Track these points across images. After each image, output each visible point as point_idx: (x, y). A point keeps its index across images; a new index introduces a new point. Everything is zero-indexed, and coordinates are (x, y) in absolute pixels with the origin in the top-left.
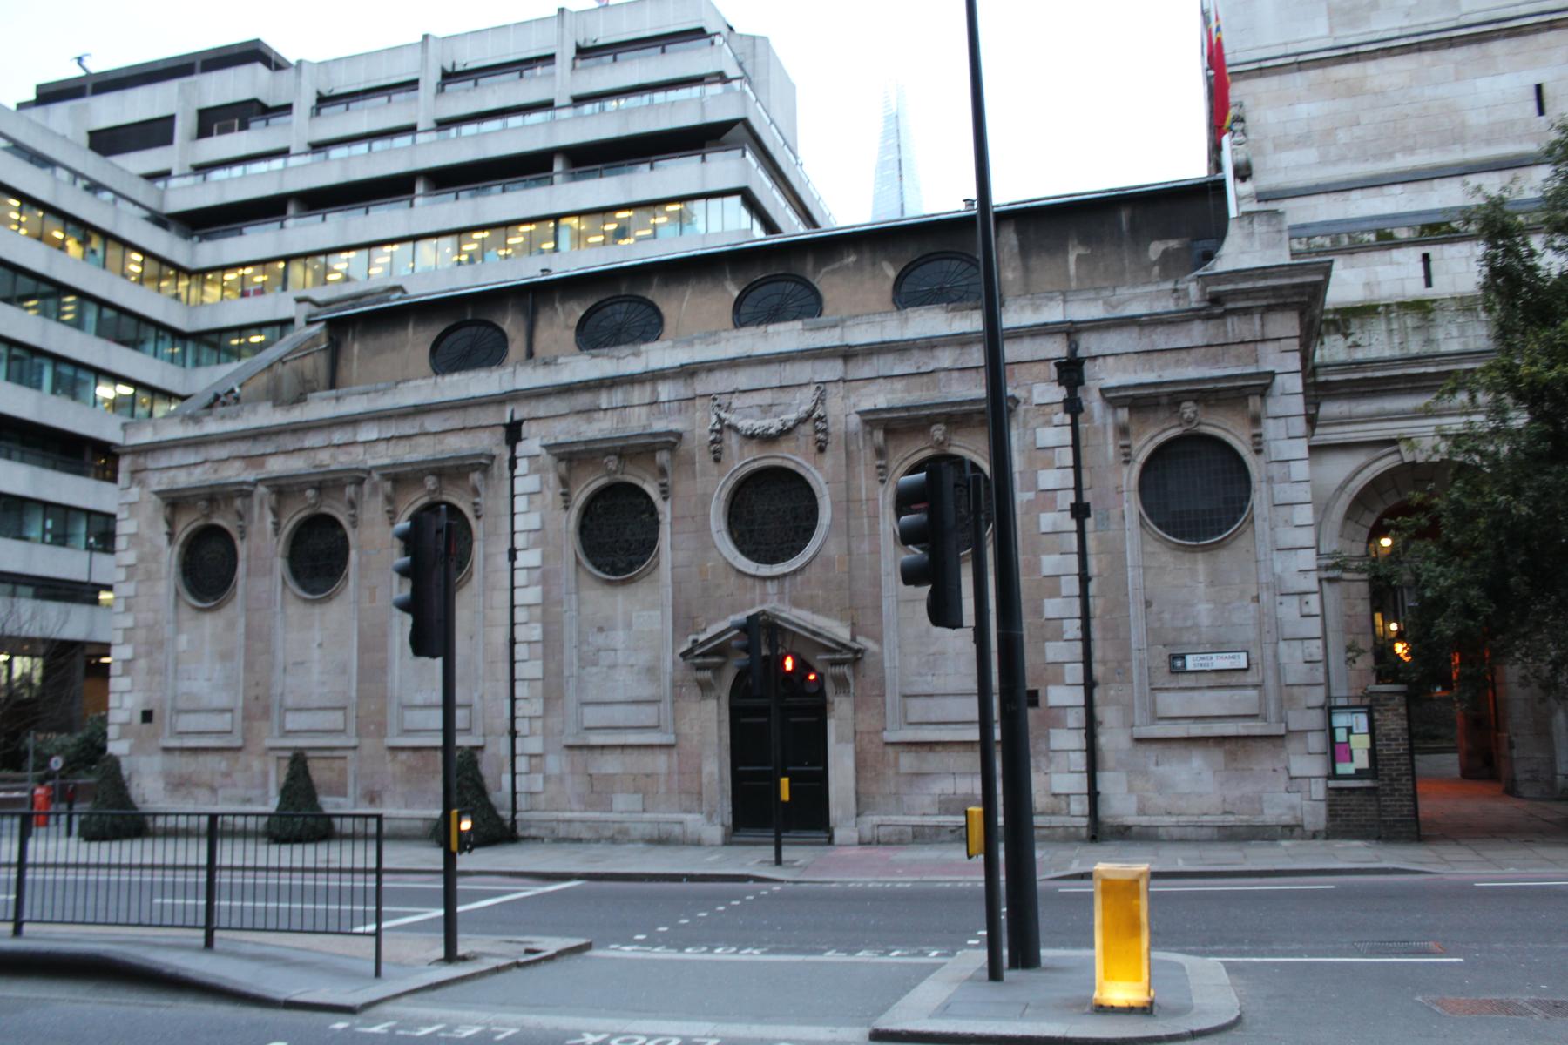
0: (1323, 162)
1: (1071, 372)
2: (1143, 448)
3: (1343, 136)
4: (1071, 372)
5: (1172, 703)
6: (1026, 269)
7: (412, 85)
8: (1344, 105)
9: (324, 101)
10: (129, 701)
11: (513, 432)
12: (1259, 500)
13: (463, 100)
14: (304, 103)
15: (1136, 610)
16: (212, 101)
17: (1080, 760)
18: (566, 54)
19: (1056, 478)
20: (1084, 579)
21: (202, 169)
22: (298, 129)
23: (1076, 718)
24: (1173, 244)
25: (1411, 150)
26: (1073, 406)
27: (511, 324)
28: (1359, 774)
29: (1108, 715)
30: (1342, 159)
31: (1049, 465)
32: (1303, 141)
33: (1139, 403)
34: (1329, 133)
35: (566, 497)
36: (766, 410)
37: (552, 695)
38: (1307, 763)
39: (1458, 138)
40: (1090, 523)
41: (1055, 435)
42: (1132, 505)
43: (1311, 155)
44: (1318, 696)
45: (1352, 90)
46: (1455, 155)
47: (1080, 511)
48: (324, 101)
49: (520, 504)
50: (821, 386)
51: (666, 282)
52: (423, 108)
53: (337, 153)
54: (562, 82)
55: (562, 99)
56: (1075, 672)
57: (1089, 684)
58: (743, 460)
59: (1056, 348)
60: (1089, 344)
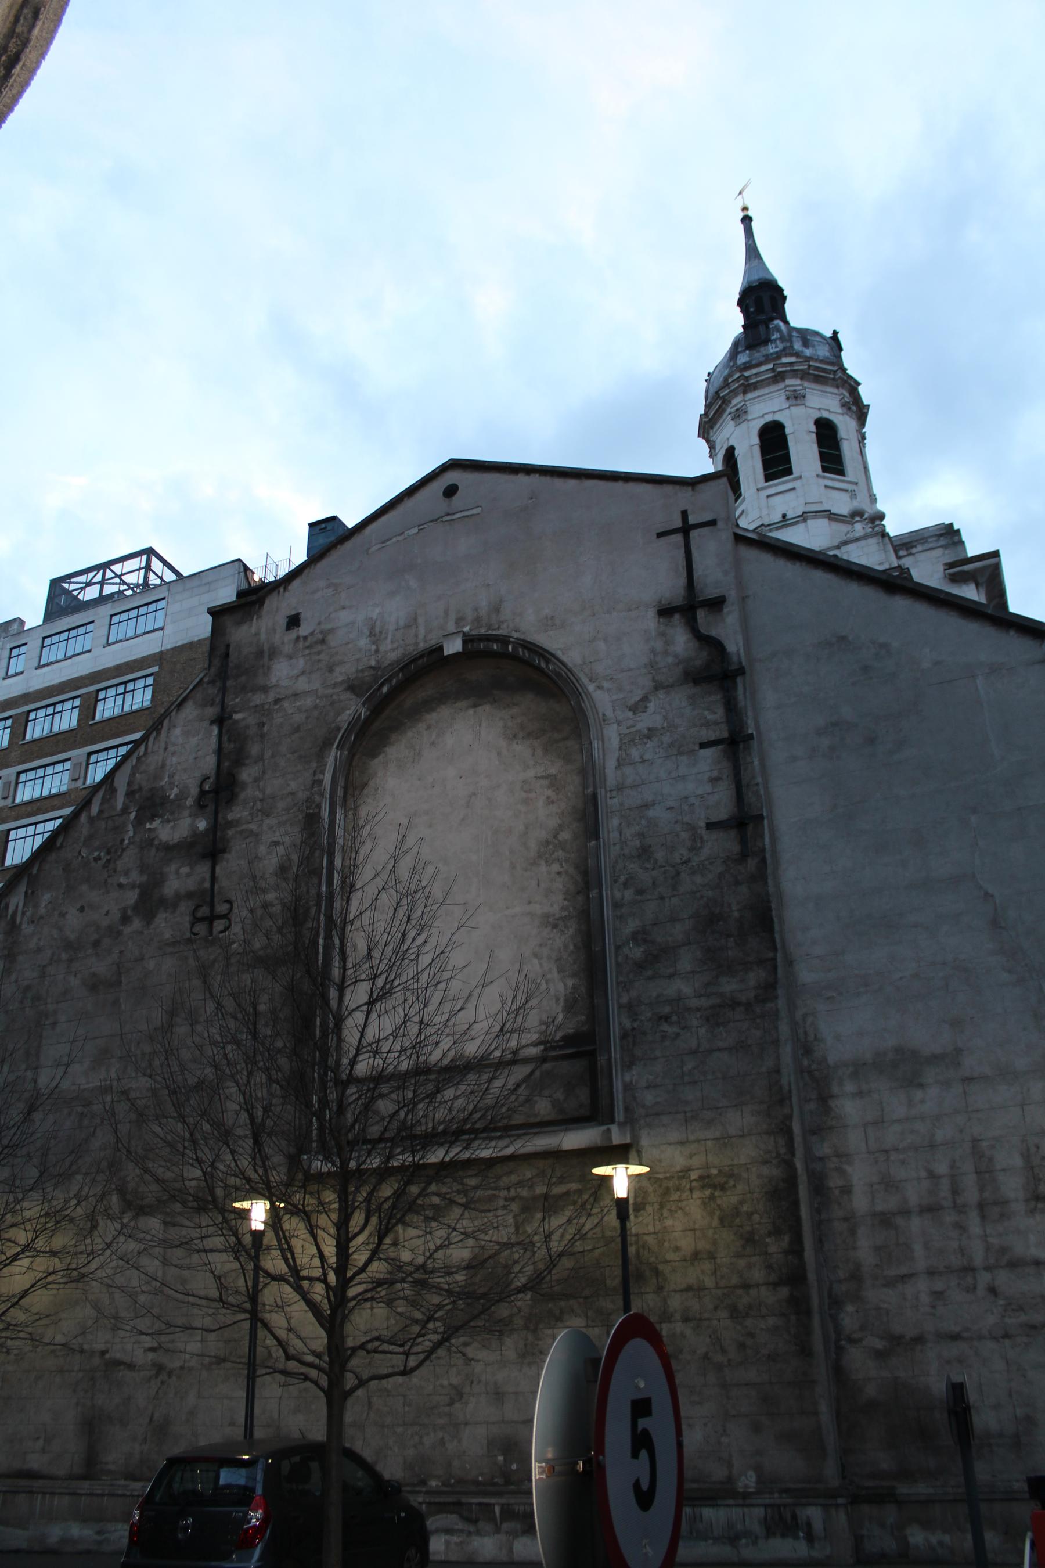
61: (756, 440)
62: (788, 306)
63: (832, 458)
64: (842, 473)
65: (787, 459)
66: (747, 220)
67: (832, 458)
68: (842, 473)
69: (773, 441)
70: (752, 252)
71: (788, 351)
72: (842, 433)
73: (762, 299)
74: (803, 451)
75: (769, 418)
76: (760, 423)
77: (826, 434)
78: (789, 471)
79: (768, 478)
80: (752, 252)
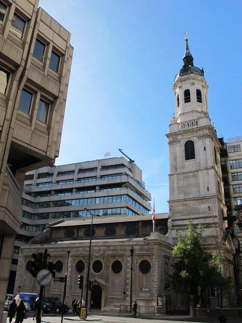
0: (181, 216)
1: (132, 251)
2: (139, 261)
3: (184, 212)
4: (132, 251)
5: (140, 294)
6: (142, 229)
7: (73, 172)
8: (185, 207)
9: (60, 174)
10: (17, 285)
11: (69, 252)
12: (151, 269)
13: (82, 175)
14: (56, 174)
15: (137, 283)
16: (40, 172)
17: (129, 301)
18: (99, 168)
19: (129, 265)
20: (132, 278)
21: (38, 184)
22: (55, 178)
23: (129, 296)
24: (161, 227)
25: (193, 215)
26: (132, 255)
27: (75, 231)
28: (161, 306)
29: (133, 296)
30: (184, 215)
31: (128, 263)
32: (179, 212)
33: (139, 256)
34: (183, 211)
35: (74, 262)
36: (98, 253)
37: (70, 288)
38: (155, 304)
39: (199, 213)
40: (133, 271)
41: (129, 259)
42: (138, 269)
43: (180, 214)
44: (156, 295)
45: (186, 205)
46: (198, 216)
47: (132, 269)
48: (60, 174)
49: (69, 262)
50: (104, 250)
51: (96, 227)
52: (76, 176)
53: (61, 184)
54: (99, 173)
55: (98, 176)
56: (130, 290)
57: (131, 291)
58: (94, 260)
59: (130, 248)
60: (135, 247)
61: (183, 92)
62: (194, 61)
63: (199, 99)
64: (201, 102)
65: (189, 98)
66: (187, 40)
67: (199, 99)
68: (201, 102)
69: (187, 93)
70: (187, 49)
71: (192, 73)
72: (202, 93)
73: (188, 60)
74: (193, 96)
75: (186, 88)
76: (184, 90)
77: (199, 93)
78: (190, 101)
79: (185, 102)
80: (187, 49)
